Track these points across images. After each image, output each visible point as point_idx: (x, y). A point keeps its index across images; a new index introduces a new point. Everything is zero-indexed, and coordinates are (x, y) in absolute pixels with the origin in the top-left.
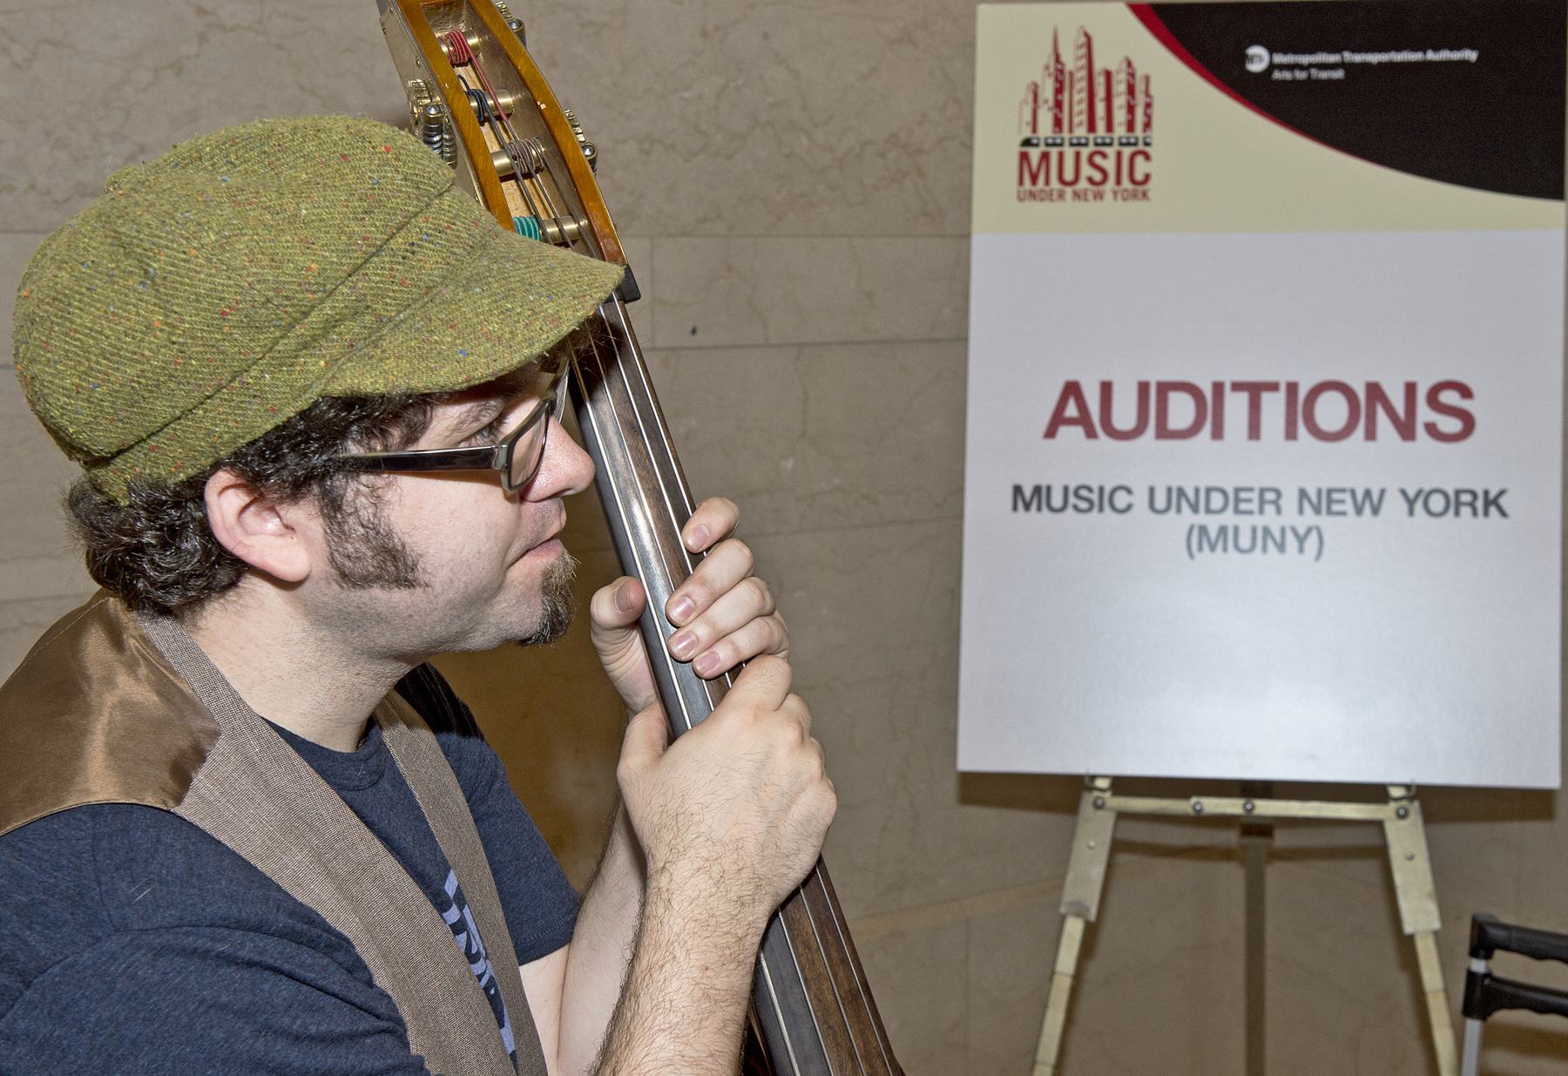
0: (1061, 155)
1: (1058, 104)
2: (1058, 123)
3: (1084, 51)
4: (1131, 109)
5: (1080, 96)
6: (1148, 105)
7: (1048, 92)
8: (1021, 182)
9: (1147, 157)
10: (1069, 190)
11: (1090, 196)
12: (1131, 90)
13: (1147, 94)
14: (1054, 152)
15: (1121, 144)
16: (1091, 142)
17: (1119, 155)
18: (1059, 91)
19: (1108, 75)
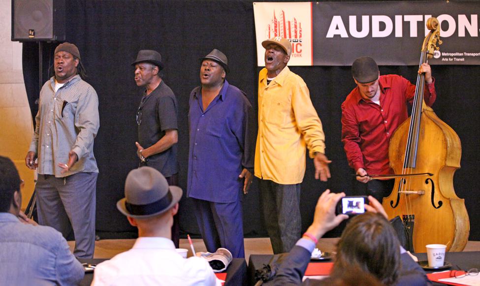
1: (276, 30)
3: (282, 16)
4: (296, 32)
5: (282, 28)
6: (301, 31)
9: (301, 45)
12: (296, 27)
13: (300, 28)
19: (289, 22)
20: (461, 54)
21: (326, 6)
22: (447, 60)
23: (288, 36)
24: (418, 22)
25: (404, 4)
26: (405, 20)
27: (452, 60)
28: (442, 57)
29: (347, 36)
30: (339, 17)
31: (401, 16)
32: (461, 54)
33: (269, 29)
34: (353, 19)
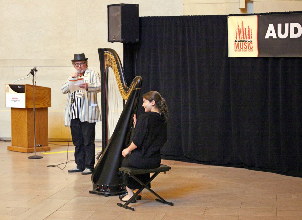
0: (240, 43)
5: (242, 33)
6: (251, 34)
9: (252, 44)
10: (242, 49)
13: (251, 32)
14: (239, 42)
17: (248, 43)
18: (239, 32)
19: (246, 29)
23: (245, 38)
30: (273, 24)
34: (280, 26)
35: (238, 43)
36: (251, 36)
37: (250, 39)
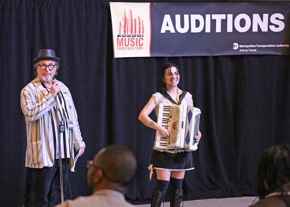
0: (125, 39)
1: (125, 27)
2: (125, 31)
3: (130, 14)
4: (140, 28)
5: (130, 25)
7: (123, 24)
8: (117, 46)
9: (143, 40)
10: (127, 47)
11: (131, 49)
13: (143, 25)
14: (124, 38)
15: (138, 36)
16: (131, 36)
17: (137, 38)
18: (125, 24)
19: (135, 20)
20: (254, 46)
21: (160, 5)
22: (243, 50)
24: (222, 20)
25: (211, 5)
26: (212, 19)
27: (247, 50)
28: (239, 48)
29: (174, 32)
31: (209, 15)
32: (254, 46)
33: (120, 26)
34: (178, 17)
35: (122, 39)
36: (143, 30)
37: (141, 34)
